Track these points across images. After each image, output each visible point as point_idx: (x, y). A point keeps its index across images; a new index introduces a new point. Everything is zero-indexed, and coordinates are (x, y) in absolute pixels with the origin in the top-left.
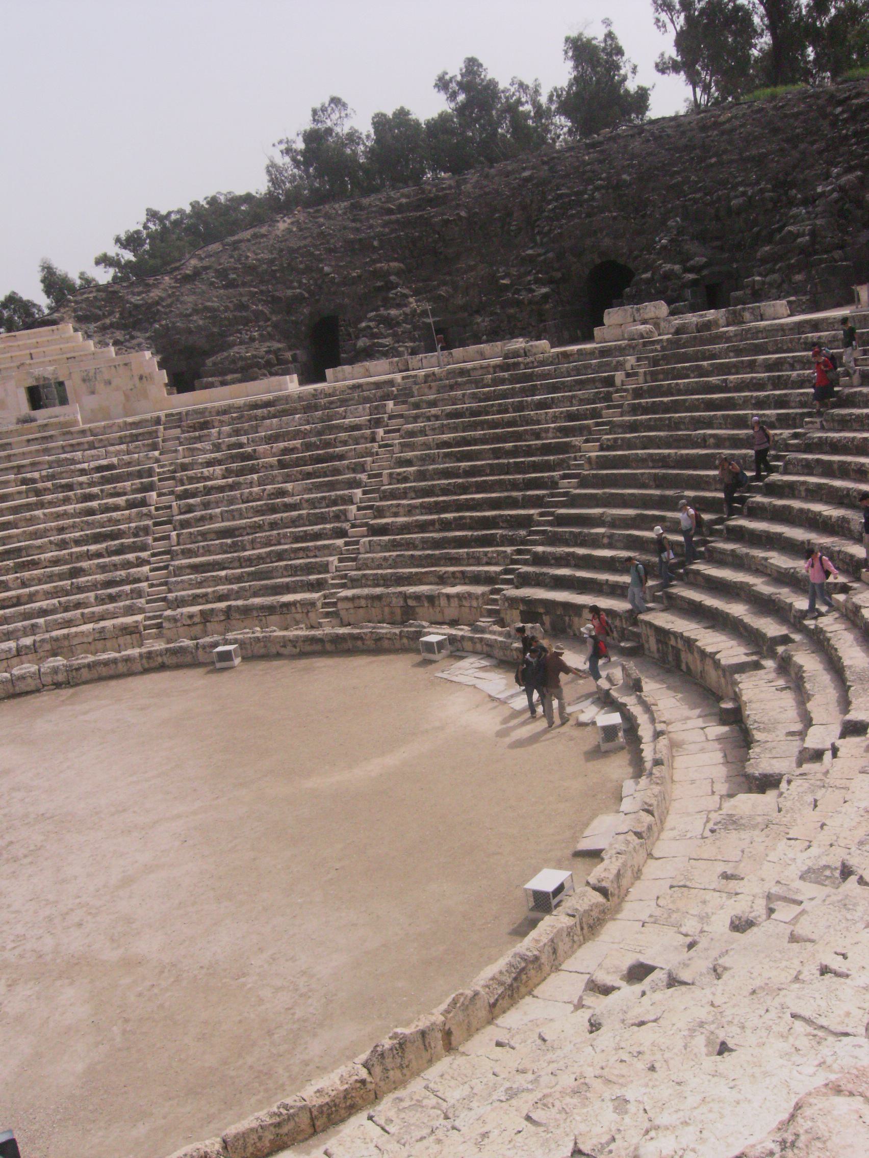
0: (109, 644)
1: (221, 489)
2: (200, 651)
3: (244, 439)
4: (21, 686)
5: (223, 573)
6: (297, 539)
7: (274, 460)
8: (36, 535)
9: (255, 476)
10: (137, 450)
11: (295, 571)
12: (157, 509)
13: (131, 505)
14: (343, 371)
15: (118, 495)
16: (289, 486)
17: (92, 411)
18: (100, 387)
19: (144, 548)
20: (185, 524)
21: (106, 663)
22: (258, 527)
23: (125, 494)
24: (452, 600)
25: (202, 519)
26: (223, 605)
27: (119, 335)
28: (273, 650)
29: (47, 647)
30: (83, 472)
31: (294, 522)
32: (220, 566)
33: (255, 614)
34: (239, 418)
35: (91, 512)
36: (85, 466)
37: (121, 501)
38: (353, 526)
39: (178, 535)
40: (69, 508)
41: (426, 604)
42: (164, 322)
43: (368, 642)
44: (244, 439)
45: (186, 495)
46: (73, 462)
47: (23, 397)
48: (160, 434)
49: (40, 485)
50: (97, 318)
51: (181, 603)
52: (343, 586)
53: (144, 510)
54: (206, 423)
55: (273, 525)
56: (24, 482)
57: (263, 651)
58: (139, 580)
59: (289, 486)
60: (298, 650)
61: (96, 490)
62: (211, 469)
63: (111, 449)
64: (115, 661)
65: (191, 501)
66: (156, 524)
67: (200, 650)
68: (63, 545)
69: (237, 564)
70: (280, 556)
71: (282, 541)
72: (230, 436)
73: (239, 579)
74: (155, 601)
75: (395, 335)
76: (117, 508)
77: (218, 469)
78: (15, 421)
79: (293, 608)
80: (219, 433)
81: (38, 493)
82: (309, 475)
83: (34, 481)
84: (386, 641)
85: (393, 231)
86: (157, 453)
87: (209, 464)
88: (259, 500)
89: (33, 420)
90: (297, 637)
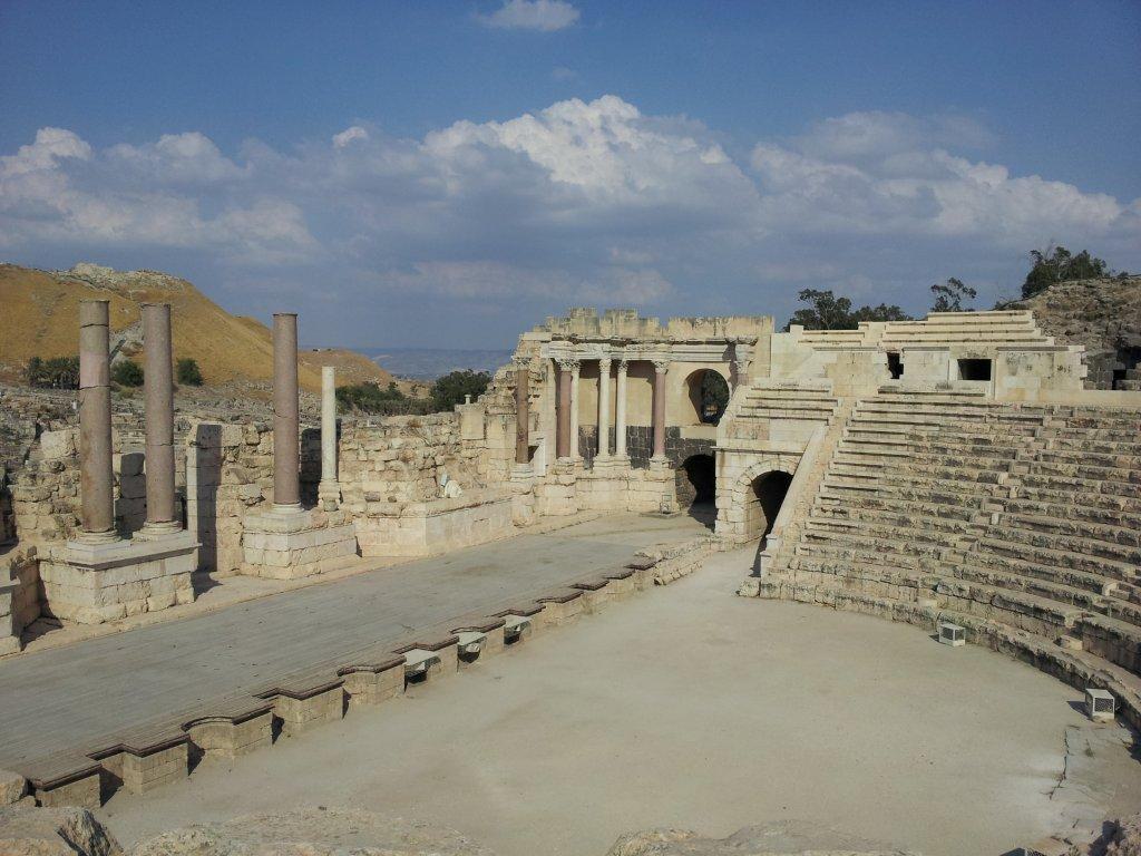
0: (892, 588)
1: (1064, 486)
3: (1113, 445)
4: (799, 595)
5: (1012, 562)
6: (1097, 552)
7: (1126, 472)
8: (893, 482)
9: (1099, 483)
10: (1017, 433)
11: (1074, 581)
12: (1001, 488)
13: (980, 480)
15: (978, 467)
16: (1122, 502)
17: (1010, 389)
18: (1022, 372)
19: (968, 519)
20: (1014, 508)
21: (865, 603)
22: (1069, 530)
23: (984, 468)
25: (1028, 508)
26: (990, 590)
27: (1076, 325)
29: (844, 573)
30: (962, 440)
31: (1103, 536)
32: (1018, 555)
33: (1013, 607)
34: (1124, 423)
35: (947, 476)
36: (966, 436)
37: (976, 473)
39: (1000, 516)
40: (931, 469)
42: (1119, 321)
44: (1113, 445)
45: (1031, 483)
46: (960, 429)
47: (955, 368)
48: (1045, 424)
49: (920, 444)
50: (1065, 308)
51: (965, 575)
52: (1104, 612)
53: (988, 486)
54: (1092, 421)
55: (1085, 533)
56: (912, 437)
58: (946, 544)
59: (1122, 502)
61: (961, 458)
62: (1066, 465)
63: (997, 426)
64: (873, 603)
65: (1030, 490)
66: (992, 501)
68: (909, 496)
70: (1071, 563)
71: (1083, 550)
72: (1104, 439)
73: (1025, 572)
74: (947, 566)
76: (968, 478)
77: (1073, 468)
78: (934, 385)
80: (1097, 434)
81: (918, 449)
83: (921, 438)
86: (1031, 439)
87: (1069, 460)
88: (1090, 505)
89: (948, 387)
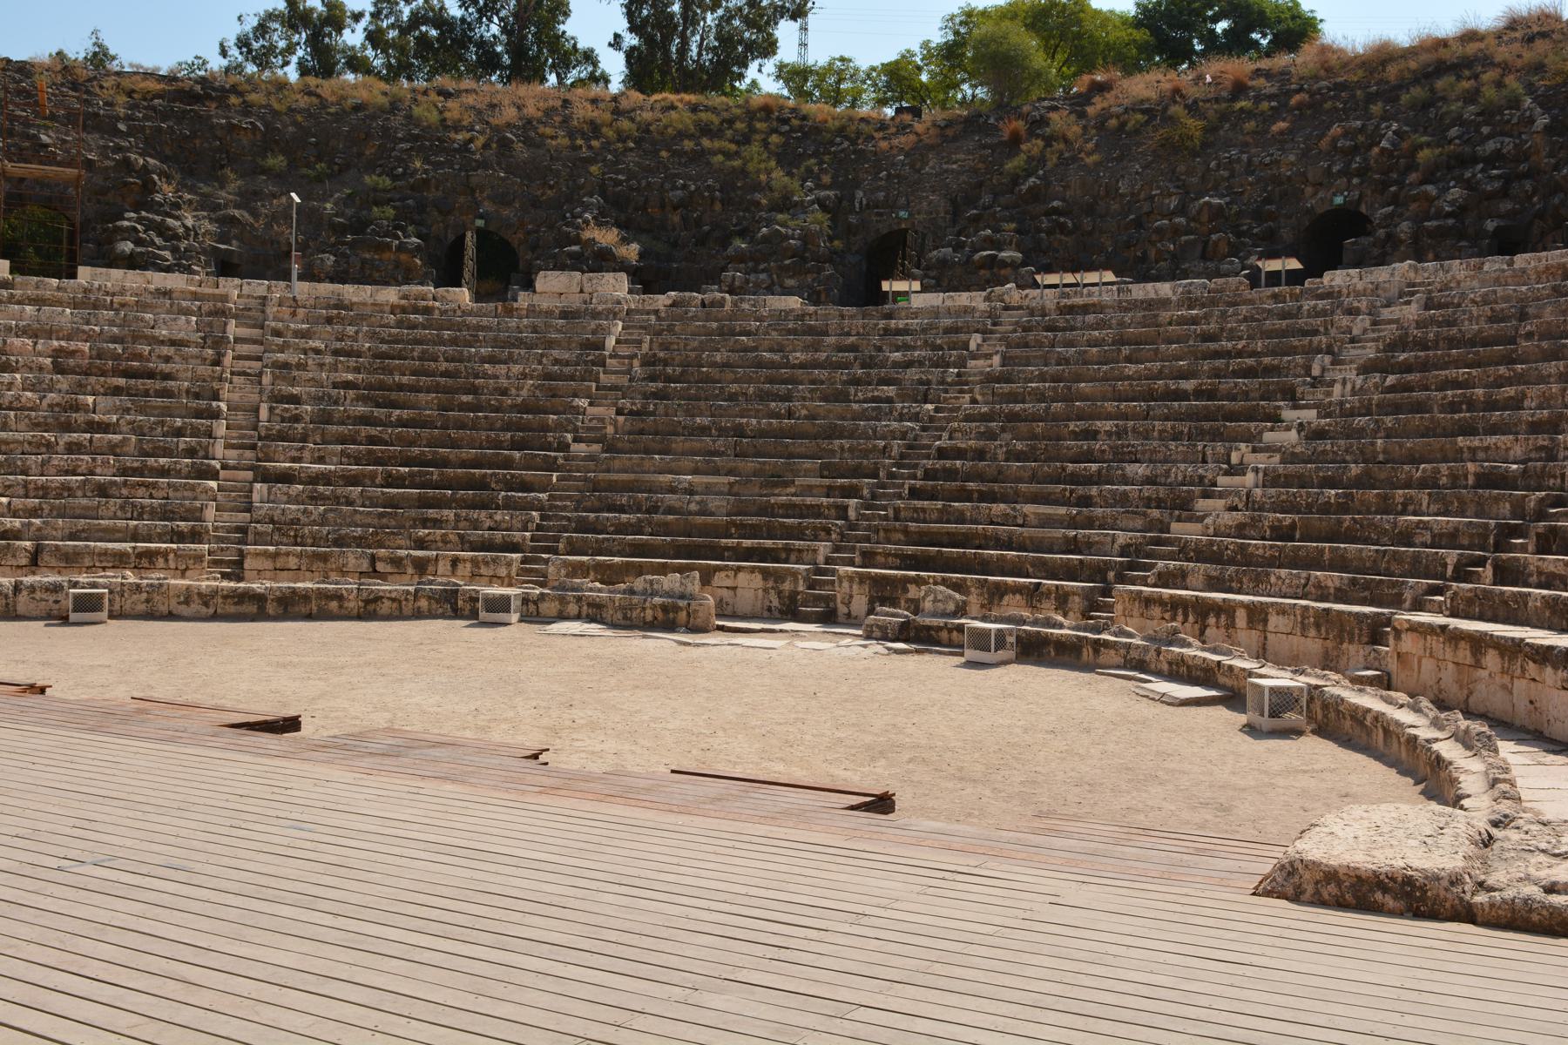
2: (23, 597)
14: (108, 275)
24: (460, 566)
28: (164, 609)
31: (113, 449)
38: (224, 467)
41: (410, 570)
43: (352, 605)
57: (142, 607)
60: (211, 611)
67: (25, 593)
69: (21, 492)
71: (98, 470)
75: (175, 250)
79: (161, 560)
82: (117, 391)
84: (387, 603)
85: (146, 118)
90: (215, 592)
